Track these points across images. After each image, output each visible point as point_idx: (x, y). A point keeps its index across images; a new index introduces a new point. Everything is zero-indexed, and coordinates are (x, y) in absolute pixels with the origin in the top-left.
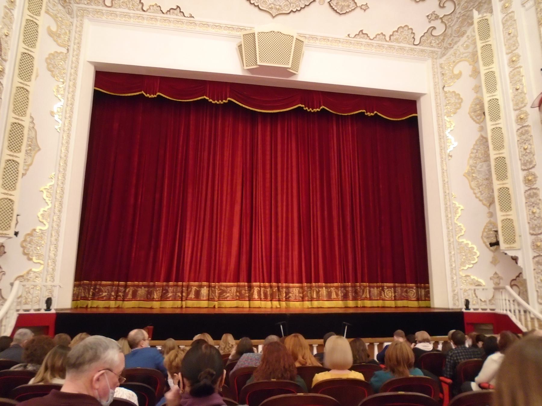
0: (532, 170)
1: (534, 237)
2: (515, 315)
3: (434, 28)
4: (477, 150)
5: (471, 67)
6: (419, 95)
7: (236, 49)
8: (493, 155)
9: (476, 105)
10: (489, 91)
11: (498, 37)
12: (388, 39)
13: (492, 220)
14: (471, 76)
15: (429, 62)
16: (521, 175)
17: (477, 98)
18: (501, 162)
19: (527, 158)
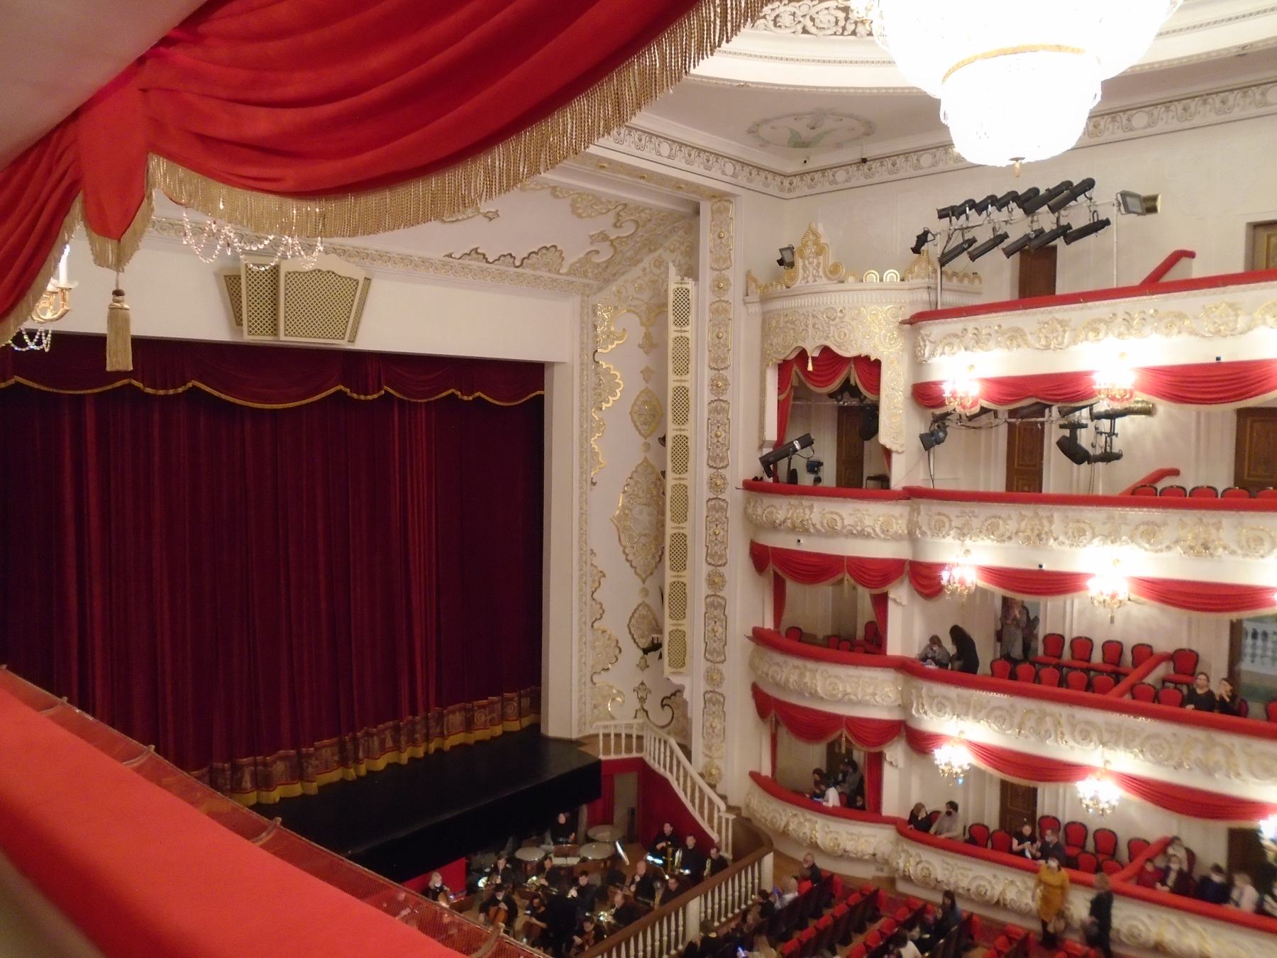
0: (721, 569)
1: (709, 664)
2: (678, 779)
3: (597, 252)
4: (637, 483)
5: (643, 330)
6: (552, 364)
7: (216, 275)
8: (670, 528)
9: (645, 403)
10: (675, 421)
11: (697, 332)
12: (518, 263)
13: (648, 601)
14: (640, 346)
15: (578, 299)
16: (705, 569)
17: (646, 391)
18: (681, 539)
19: (716, 548)
